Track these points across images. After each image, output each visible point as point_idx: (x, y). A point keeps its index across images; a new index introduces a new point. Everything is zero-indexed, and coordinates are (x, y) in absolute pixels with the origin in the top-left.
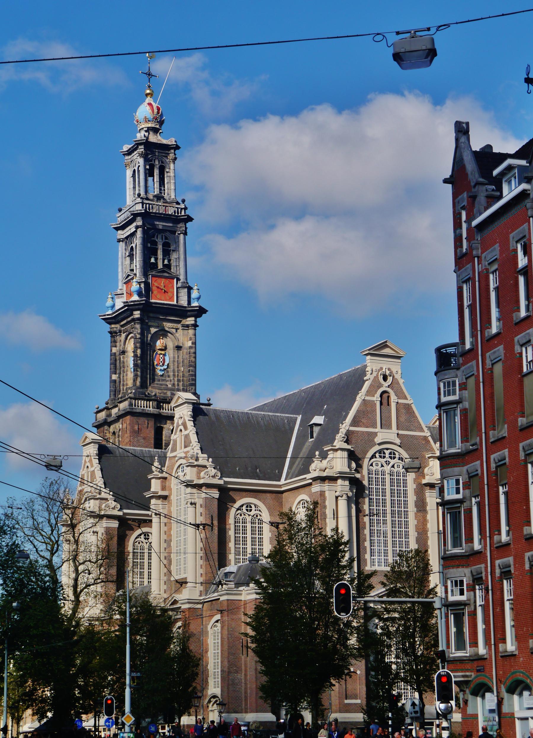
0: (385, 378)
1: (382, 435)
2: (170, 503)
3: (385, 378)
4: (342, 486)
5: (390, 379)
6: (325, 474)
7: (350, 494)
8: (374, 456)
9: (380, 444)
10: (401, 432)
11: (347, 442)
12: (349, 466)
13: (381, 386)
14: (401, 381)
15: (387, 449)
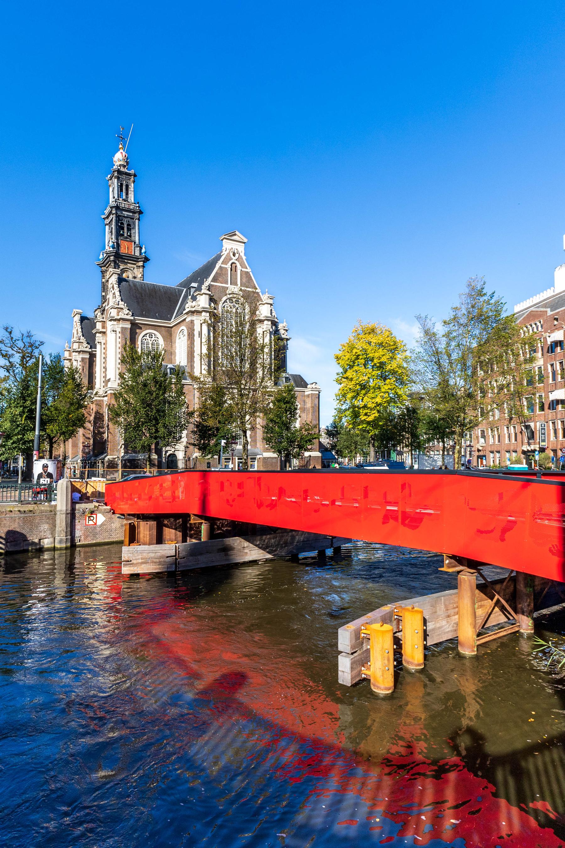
0: (234, 255)
1: (232, 289)
2: (106, 335)
3: (234, 255)
4: (205, 316)
5: (237, 255)
6: (193, 309)
7: (210, 322)
8: (225, 301)
9: (229, 294)
10: (243, 288)
11: (209, 290)
12: (210, 305)
13: (231, 259)
14: (244, 258)
15: (234, 298)
